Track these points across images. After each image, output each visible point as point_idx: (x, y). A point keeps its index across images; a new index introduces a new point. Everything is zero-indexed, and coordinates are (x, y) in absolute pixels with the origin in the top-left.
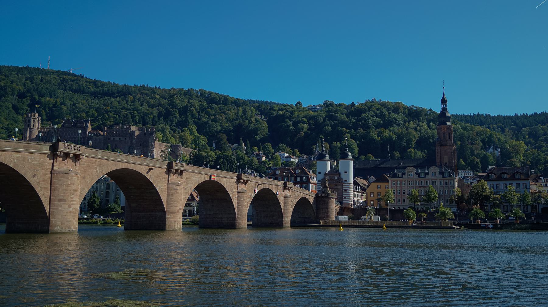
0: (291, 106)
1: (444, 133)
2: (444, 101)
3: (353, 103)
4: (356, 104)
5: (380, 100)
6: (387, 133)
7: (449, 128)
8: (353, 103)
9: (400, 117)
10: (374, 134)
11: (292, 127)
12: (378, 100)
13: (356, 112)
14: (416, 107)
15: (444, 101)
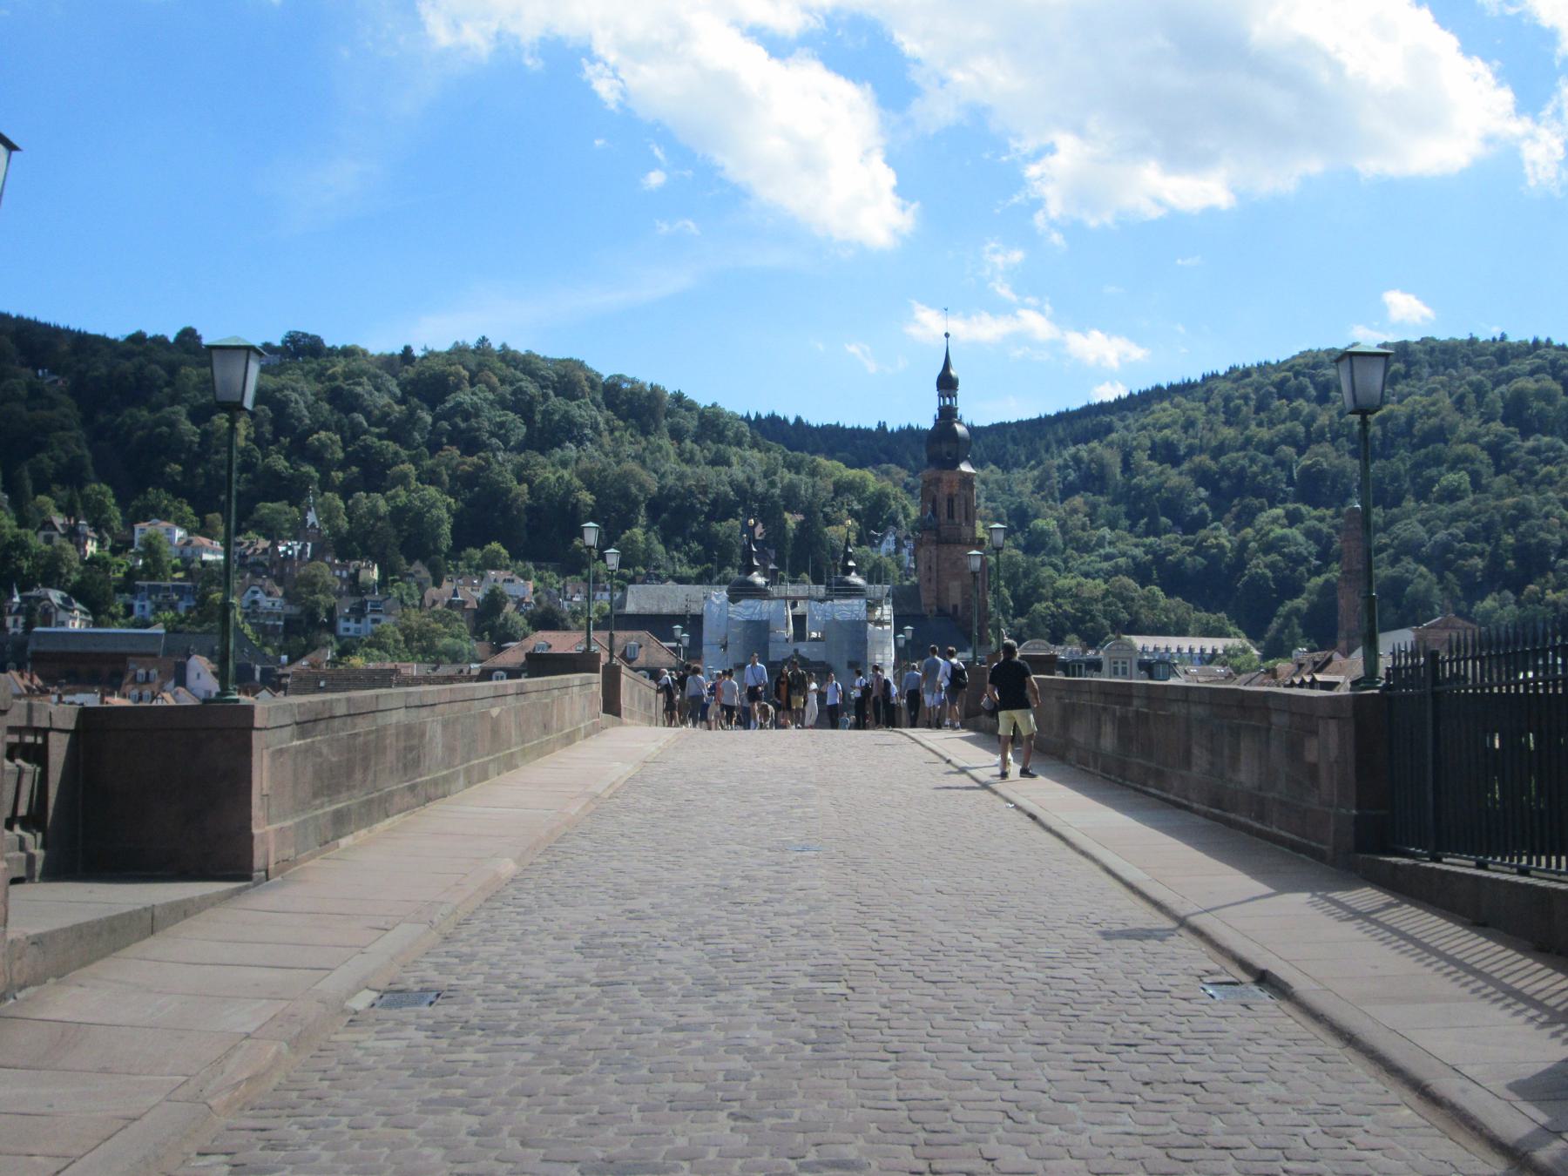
0: (160, 341)
1: (951, 500)
2: (947, 383)
3: (408, 350)
4: (418, 352)
5: (504, 346)
6: (550, 471)
7: (967, 480)
8: (408, 350)
9: (585, 411)
10: (503, 465)
11: (186, 426)
12: (496, 346)
13: (427, 381)
14: (633, 381)
15: (947, 383)
